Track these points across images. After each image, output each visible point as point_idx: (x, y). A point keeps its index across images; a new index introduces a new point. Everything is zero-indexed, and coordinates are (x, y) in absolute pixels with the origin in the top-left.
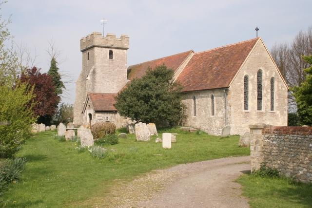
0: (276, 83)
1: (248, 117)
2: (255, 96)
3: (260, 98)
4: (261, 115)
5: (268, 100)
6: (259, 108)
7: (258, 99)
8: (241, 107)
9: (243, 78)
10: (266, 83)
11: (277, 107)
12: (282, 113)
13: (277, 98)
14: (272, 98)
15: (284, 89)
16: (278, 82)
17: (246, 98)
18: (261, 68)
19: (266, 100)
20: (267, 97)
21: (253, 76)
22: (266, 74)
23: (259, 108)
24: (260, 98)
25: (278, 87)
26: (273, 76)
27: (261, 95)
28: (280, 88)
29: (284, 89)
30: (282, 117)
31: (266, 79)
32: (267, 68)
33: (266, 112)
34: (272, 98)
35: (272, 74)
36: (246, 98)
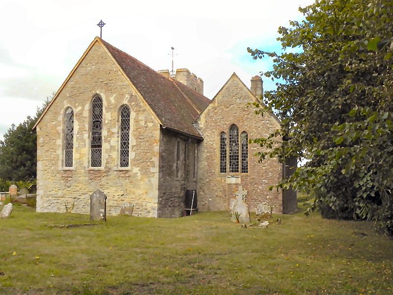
0: (133, 115)
1: (69, 179)
2: (84, 141)
3: (96, 144)
4: (94, 176)
5: (111, 146)
6: (96, 161)
7: (93, 146)
8: (56, 164)
9: (62, 112)
10: (109, 116)
11: (134, 160)
12: (146, 172)
13: (135, 144)
14: (125, 143)
15: (150, 125)
16: (138, 112)
17: (69, 146)
18: (98, 92)
19: (109, 147)
20: (109, 142)
21: (80, 108)
22: (109, 101)
23: (96, 161)
24: (96, 144)
25: (137, 121)
26: (125, 102)
27: (100, 139)
28: (142, 123)
29: (150, 125)
30: (146, 180)
31: (108, 109)
32: (109, 90)
33: (108, 170)
34: (125, 143)
35: (122, 99)
36: (69, 146)
